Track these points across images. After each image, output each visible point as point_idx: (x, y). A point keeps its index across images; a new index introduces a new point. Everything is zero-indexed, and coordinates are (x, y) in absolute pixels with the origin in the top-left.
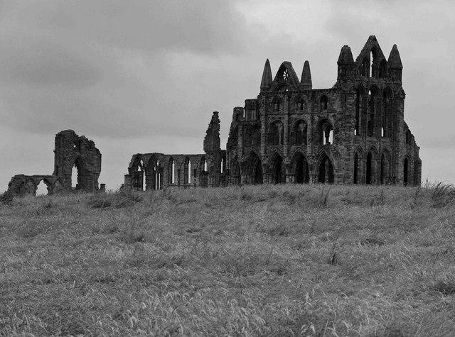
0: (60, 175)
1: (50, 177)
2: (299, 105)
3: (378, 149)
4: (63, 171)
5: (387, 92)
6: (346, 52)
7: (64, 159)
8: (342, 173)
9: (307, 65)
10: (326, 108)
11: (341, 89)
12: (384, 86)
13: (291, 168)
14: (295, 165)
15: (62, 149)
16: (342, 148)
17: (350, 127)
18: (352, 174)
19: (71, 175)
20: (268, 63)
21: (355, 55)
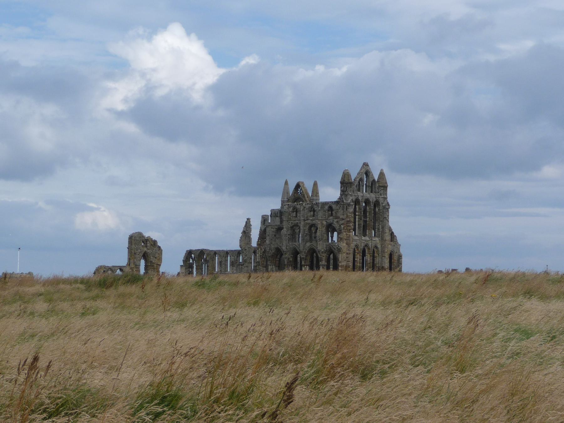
0: (132, 265)
1: (124, 267)
2: (312, 213)
3: (370, 246)
4: (134, 263)
5: (377, 204)
6: (346, 175)
7: (135, 253)
8: (344, 263)
9: (315, 184)
10: (332, 215)
11: (343, 202)
12: (375, 199)
13: (306, 259)
14: (309, 258)
15: (133, 246)
16: (343, 245)
17: (350, 229)
18: (351, 264)
19: (140, 265)
20: (286, 183)
21: (354, 176)
